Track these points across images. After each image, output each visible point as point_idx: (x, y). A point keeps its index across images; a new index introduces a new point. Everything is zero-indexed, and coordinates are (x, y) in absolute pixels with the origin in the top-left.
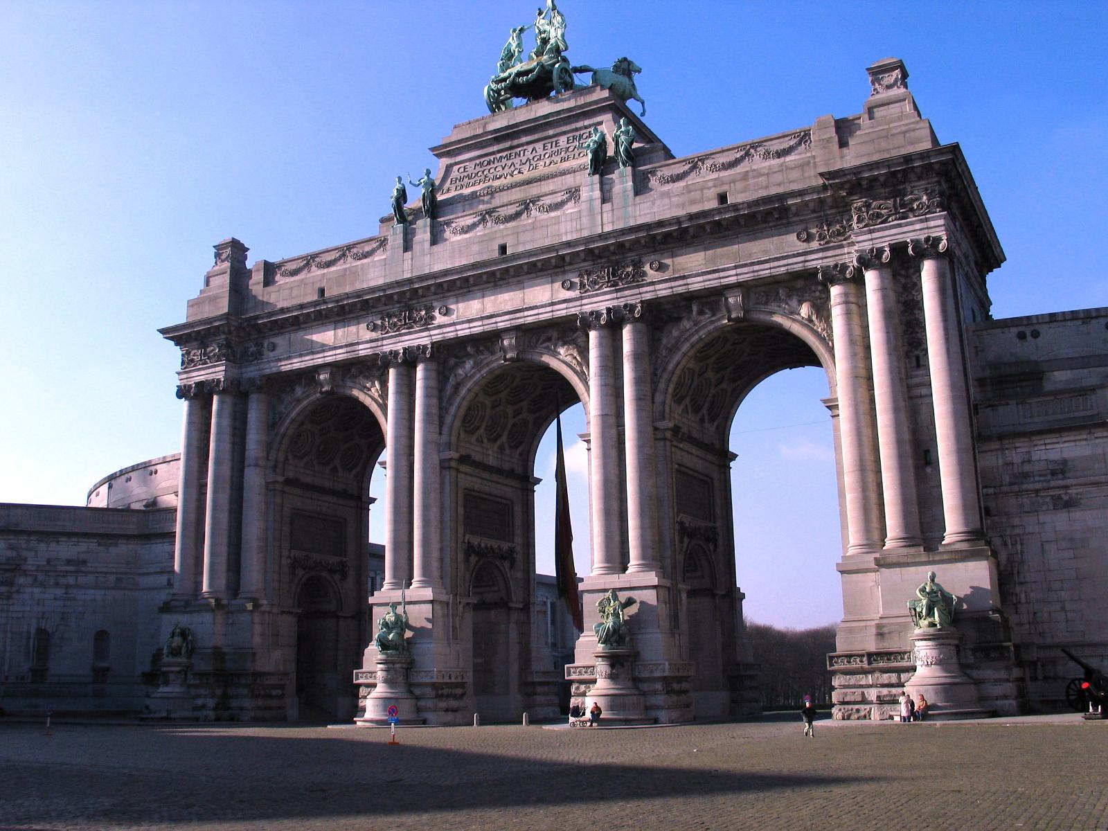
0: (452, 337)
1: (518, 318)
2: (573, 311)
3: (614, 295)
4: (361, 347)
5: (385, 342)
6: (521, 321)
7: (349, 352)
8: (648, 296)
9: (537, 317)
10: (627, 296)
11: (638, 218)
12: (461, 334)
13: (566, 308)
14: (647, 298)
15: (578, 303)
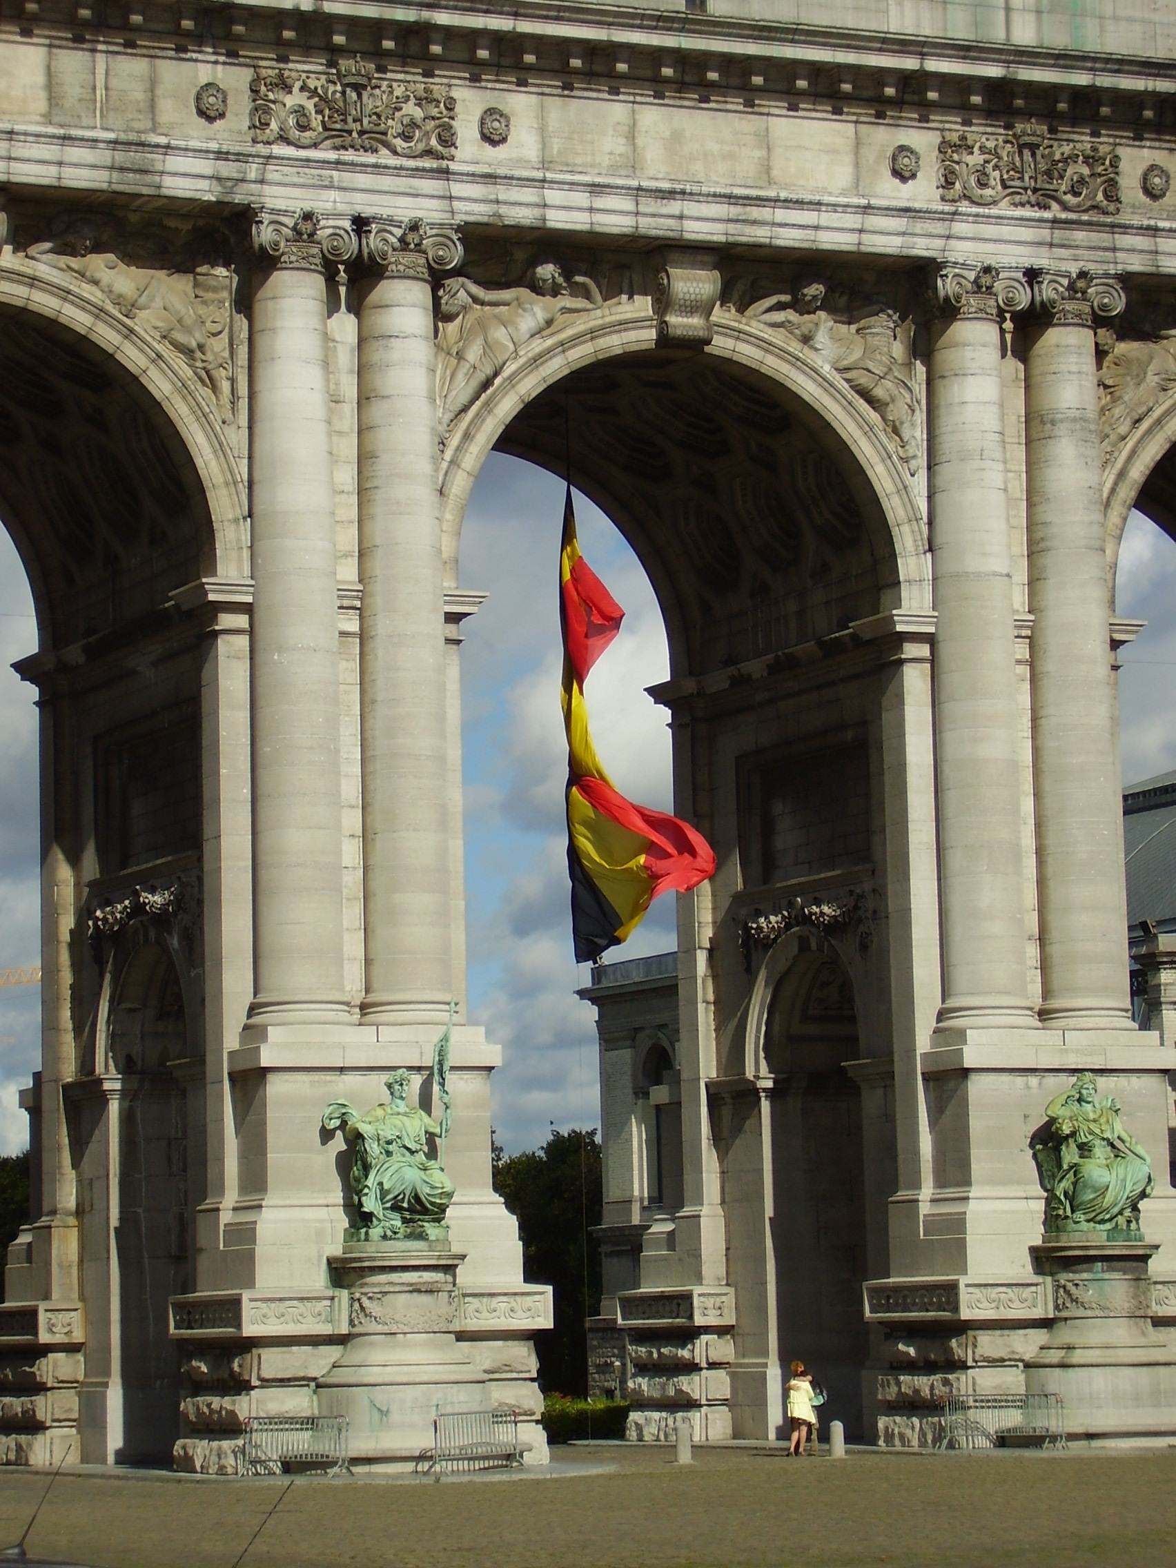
0: (526, 222)
1: (754, 222)
2: (922, 247)
3: (1045, 234)
4: (175, 163)
5: (273, 173)
6: (760, 235)
7: (122, 169)
8: (1136, 264)
9: (810, 234)
10: (1077, 247)
11: (1110, 26)
12: (558, 220)
13: (904, 234)
14: (1130, 268)
15: (939, 228)
